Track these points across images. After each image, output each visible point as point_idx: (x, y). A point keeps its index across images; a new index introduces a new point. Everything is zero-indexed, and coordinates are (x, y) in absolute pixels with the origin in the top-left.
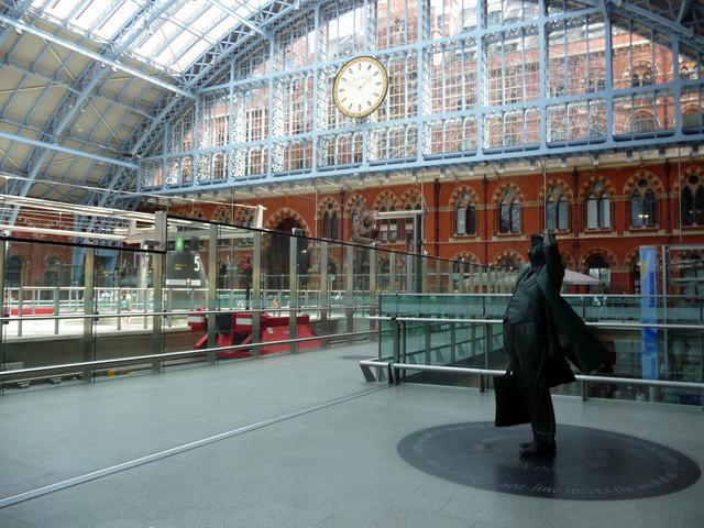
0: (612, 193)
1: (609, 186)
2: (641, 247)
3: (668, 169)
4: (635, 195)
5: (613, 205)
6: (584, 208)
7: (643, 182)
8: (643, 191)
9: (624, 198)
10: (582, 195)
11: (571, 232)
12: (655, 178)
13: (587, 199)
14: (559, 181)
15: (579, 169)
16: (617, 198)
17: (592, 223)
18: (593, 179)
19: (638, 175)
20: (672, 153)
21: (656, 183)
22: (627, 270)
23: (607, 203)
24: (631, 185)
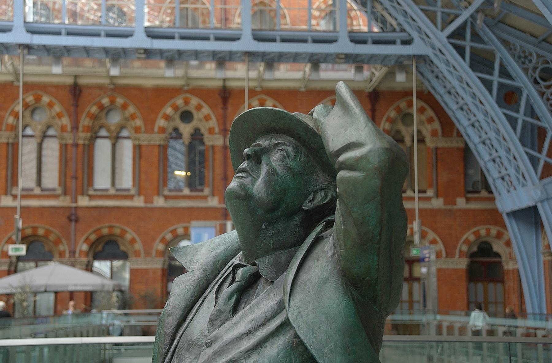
0: (137, 130)
1: (133, 117)
2: (194, 223)
3: (225, 96)
4: (177, 134)
5: (138, 150)
6: (89, 150)
7: (186, 116)
8: (186, 129)
9: (157, 139)
10: (88, 129)
11: (65, 193)
12: (206, 110)
13: (95, 137)
14: (46, 99)
15: (82, 81)
16: (144, 138)
17: (102, 181)
18: (105, 101)
19: (179, 102)
20: (239, 74)
21: (207, 118)
22: (157, 264)
23: (127, 148)
24: (167, 118)
